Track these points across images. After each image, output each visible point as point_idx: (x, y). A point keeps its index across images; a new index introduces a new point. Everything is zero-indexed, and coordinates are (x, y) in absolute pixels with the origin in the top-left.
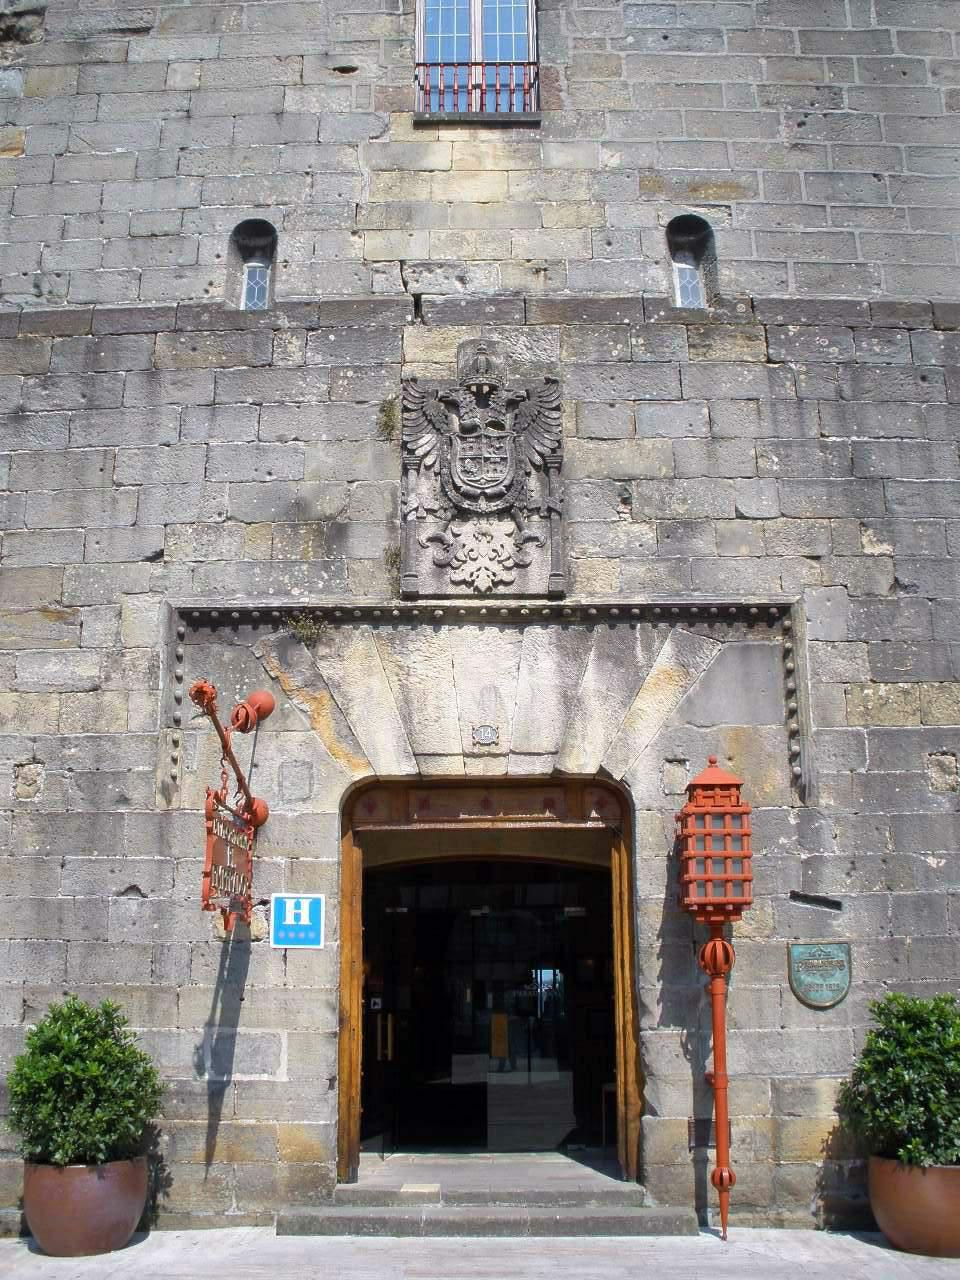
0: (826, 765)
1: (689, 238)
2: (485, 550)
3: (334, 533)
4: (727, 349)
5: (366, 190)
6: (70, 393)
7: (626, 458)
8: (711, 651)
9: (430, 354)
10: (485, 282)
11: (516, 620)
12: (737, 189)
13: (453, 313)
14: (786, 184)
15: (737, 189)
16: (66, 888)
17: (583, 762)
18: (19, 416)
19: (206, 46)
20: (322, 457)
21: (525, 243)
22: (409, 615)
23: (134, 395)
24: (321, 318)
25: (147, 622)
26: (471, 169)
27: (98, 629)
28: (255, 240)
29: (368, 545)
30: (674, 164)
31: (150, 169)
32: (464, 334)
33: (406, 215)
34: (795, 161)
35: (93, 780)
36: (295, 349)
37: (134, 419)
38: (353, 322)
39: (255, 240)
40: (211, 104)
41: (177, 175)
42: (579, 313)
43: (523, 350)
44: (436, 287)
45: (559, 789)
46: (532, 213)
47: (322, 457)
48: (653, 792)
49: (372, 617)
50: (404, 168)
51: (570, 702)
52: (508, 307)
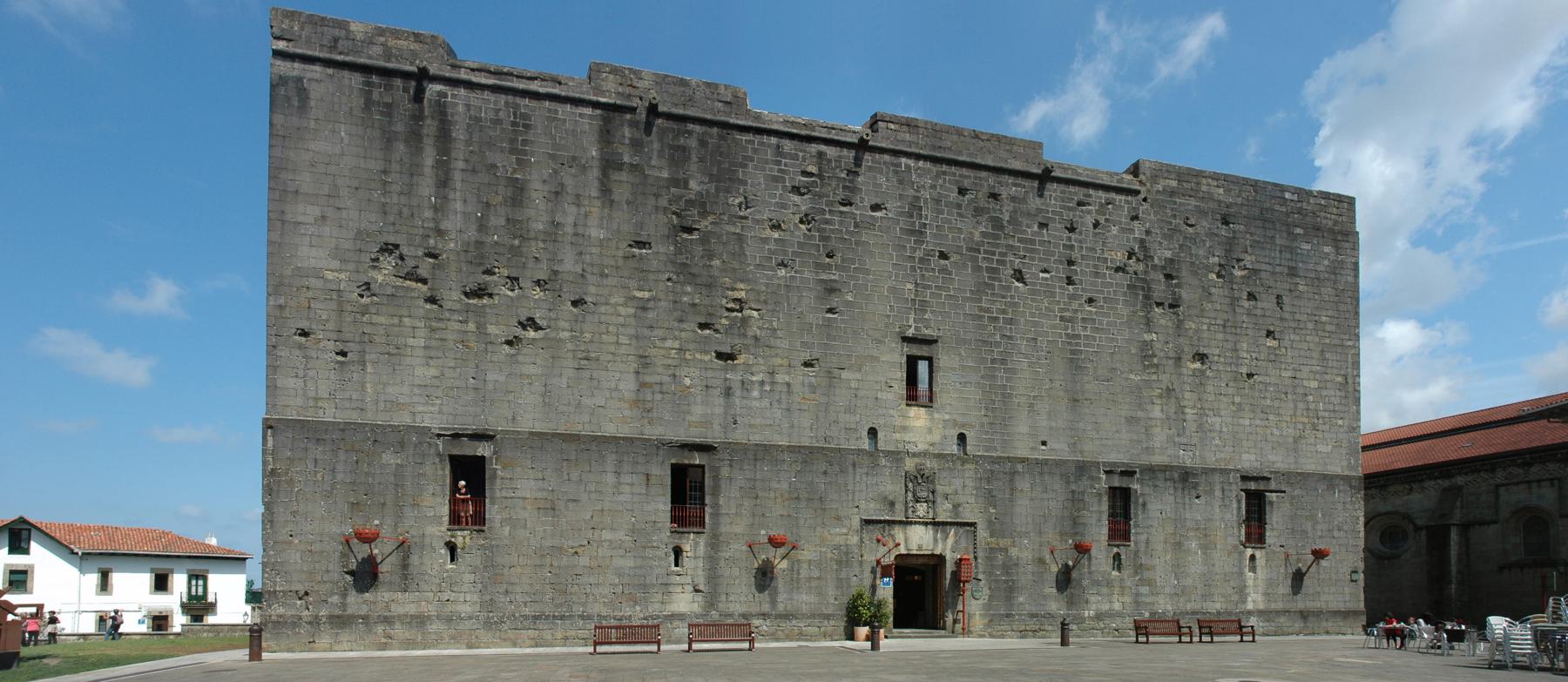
0: (980, 554)
1: (962, 438)
2: (922, 509)
3: (892, 504)
4: (968, 466)
5: (898, 422)
6: (836, 468)
7: (948, 490)
8: (961, 530)
9: (910, 464)
10: (921, 447)
11: (926, 524)
12: (972, 426)
13: (914, 455)
14: (982, 425)
15: (972, 426)
16: (843, 575)
17: (937, 552)
18: (825, 473)
19: (858, 376)
20: (889, 487)
21: (929, 438)
22: (906, 523)
23: (850, 469)
24: (888, 454)
25: (856, 522)
26: (918, 417)
27: (847, 522)
28: (873, 432)
29: (899, 507)
30: (960, 419)
31: (850, 410)
32: (917, 460)
33: (904, 429)
34: (985, 420)
35: (847, 554)
36: (883, 462)
37: (851, 477)
38: (896, 456)
39: (873, 432)
40: (861, 393)
41: (854, 413)
42: (940, 456)
43: (929, 464)
44: (912, 449)
45: (933, 555)
46: (930, 431)
47: (889, 487)
48: (951, 557)
49: (900, 522)
50: (905, 417)
51: (936, 540)
52: (924, 454)
